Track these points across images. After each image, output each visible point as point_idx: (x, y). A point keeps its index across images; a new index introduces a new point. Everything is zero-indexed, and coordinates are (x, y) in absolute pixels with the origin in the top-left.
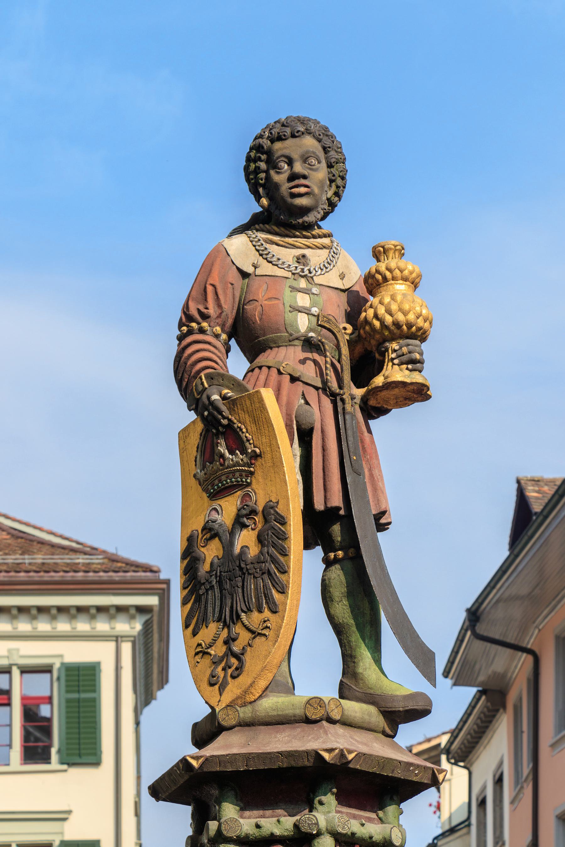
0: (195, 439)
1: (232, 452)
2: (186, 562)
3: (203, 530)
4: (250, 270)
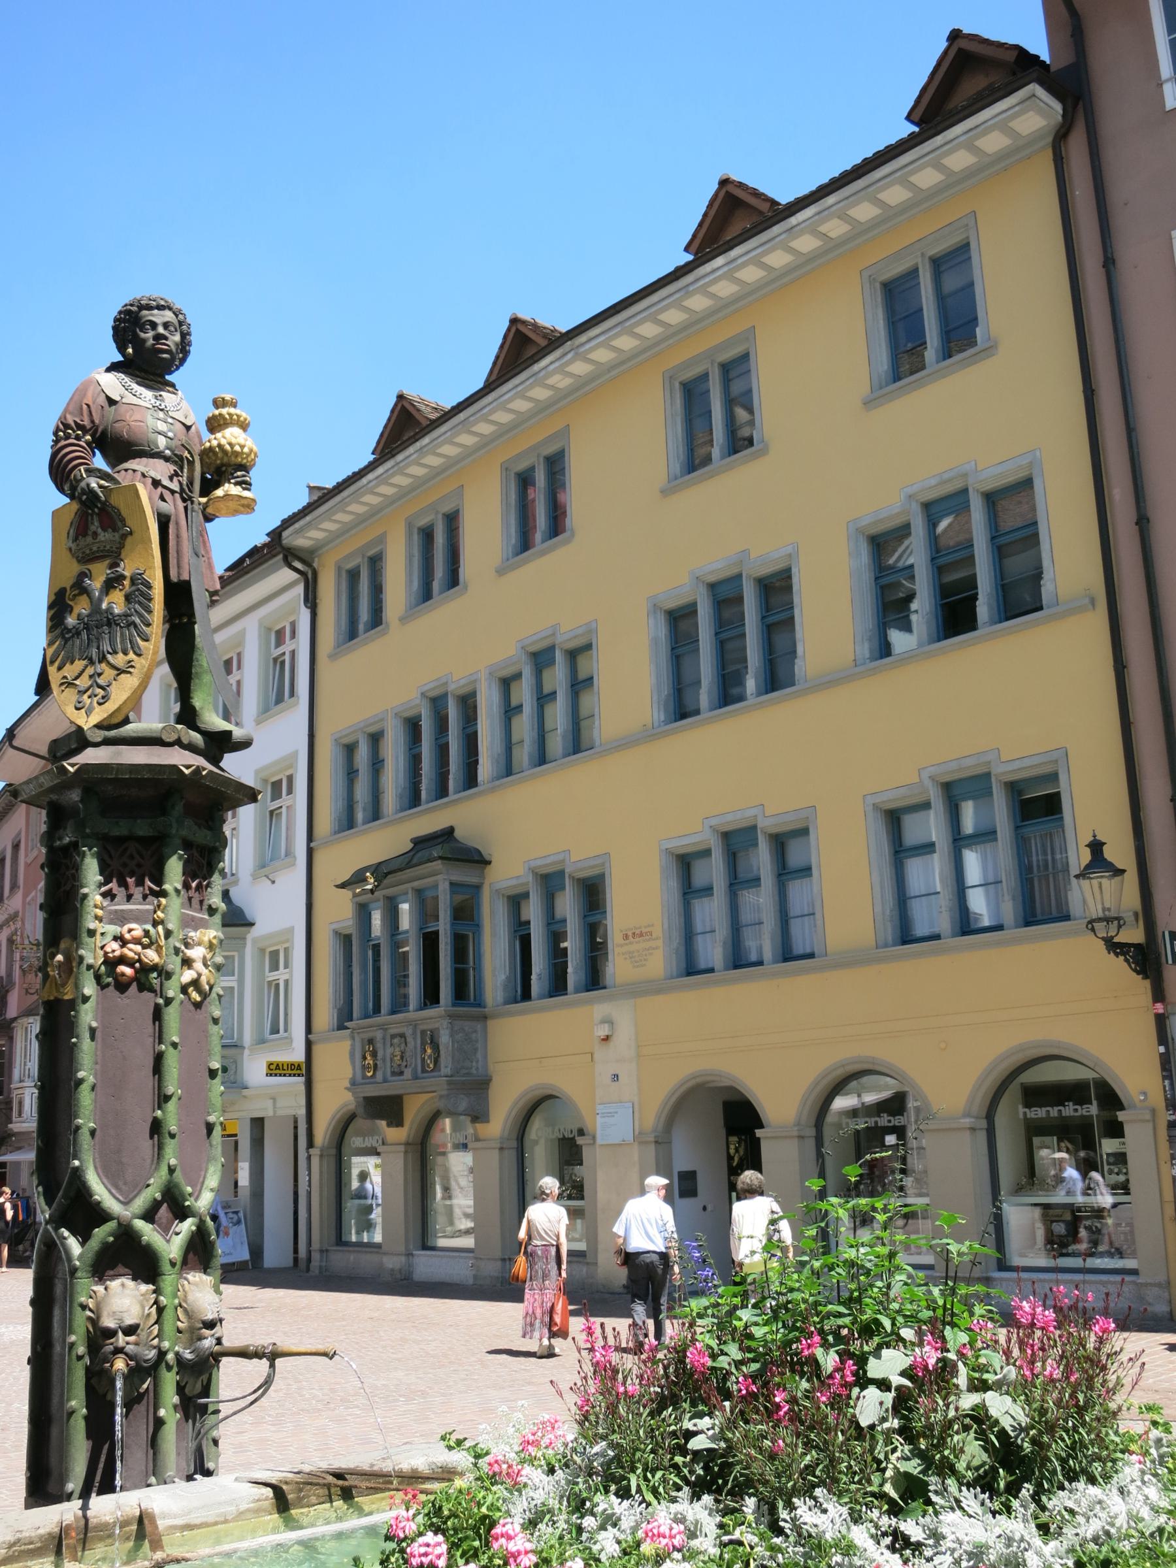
0: (69, 516)
1: (104, 530)
2: (52, 612)
3: (72, 587)
4: (117, 398)
